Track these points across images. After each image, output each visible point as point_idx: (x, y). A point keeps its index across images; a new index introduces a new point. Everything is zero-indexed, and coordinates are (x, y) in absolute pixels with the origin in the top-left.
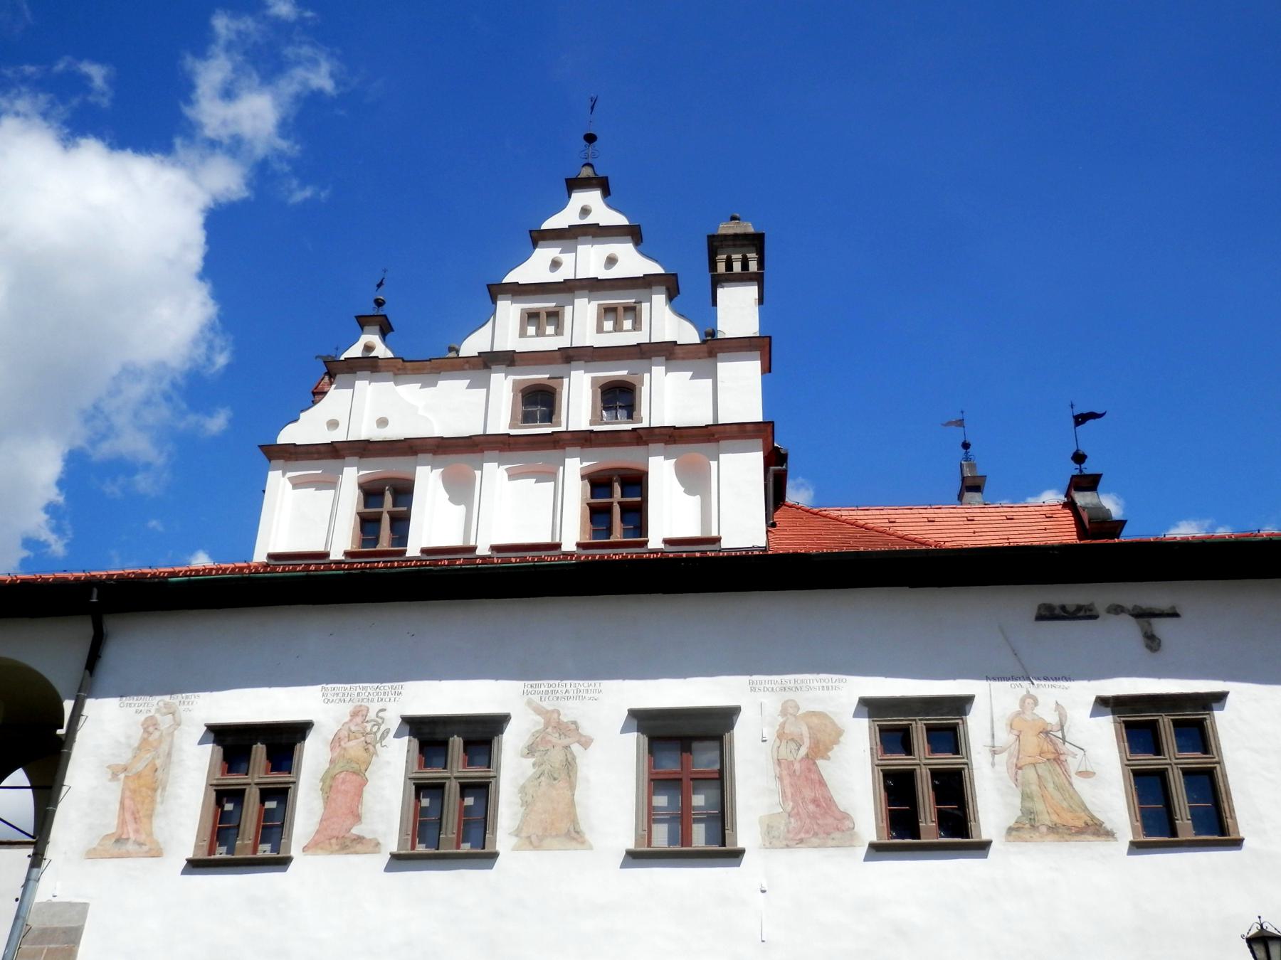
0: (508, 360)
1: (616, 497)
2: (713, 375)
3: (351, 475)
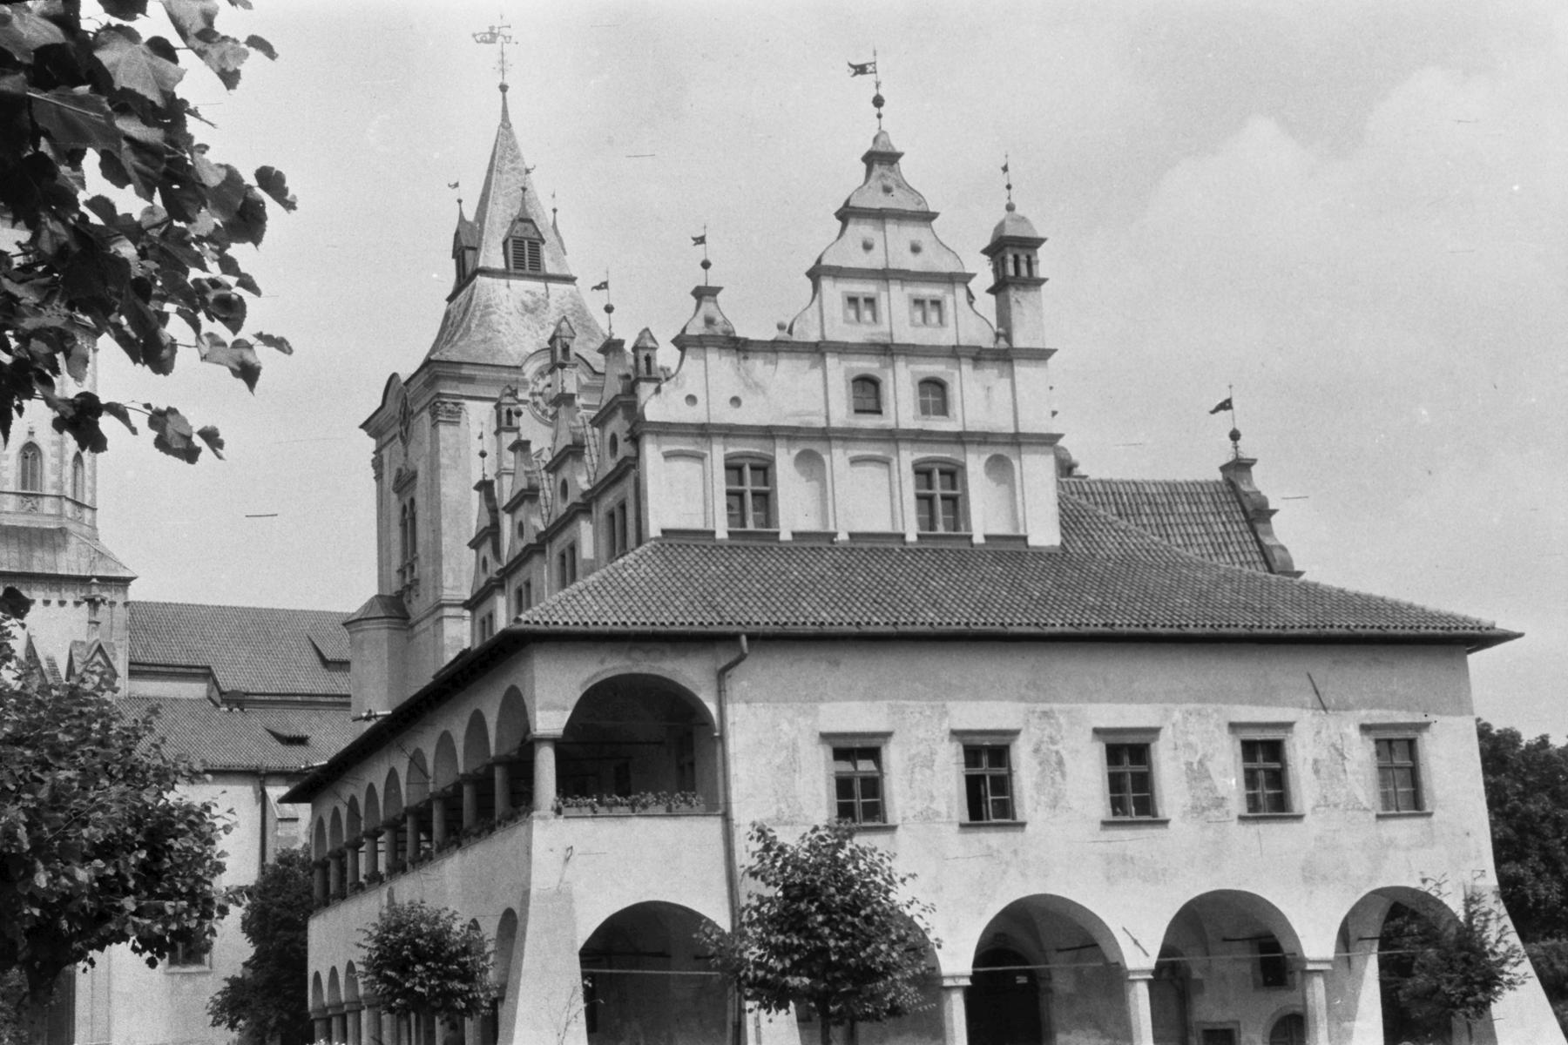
0: (843, 349)
1: (941, 489)
2: (1012, 376)
3: (718, 453)
